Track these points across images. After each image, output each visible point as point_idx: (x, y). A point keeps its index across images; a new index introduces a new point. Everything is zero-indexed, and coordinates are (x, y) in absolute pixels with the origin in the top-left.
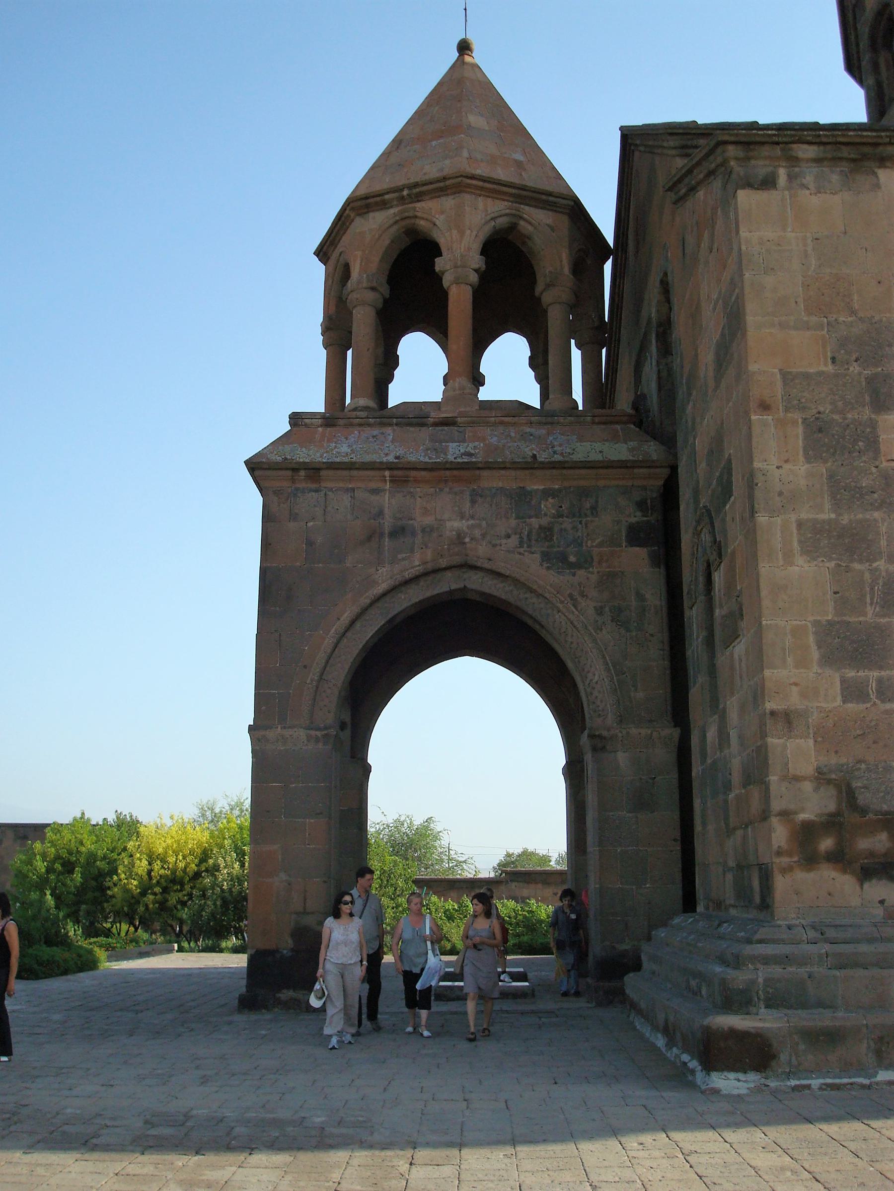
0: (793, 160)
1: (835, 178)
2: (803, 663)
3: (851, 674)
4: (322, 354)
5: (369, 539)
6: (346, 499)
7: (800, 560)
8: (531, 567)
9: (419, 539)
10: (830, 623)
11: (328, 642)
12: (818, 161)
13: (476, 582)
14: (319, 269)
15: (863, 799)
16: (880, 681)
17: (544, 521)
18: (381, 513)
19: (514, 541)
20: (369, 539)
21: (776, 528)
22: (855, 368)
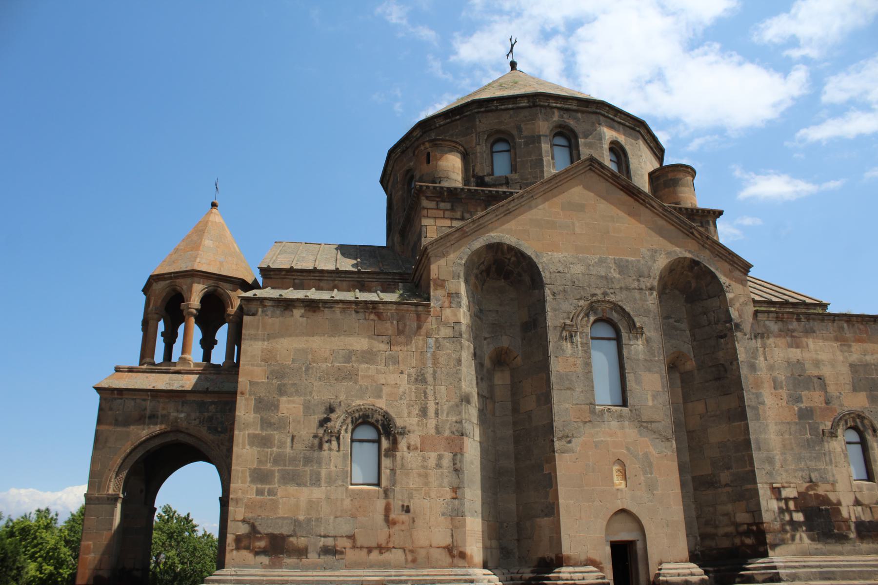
0: (265, 306)
1: (278, 312)
2: (243, 482)
3: (259, 486)
4: (140, 334)
5: (140, 419)
6: (132, 403)
7: (248, 447)
8: (204, 432)
9: (159, 420)
10: (255, 469)
11: (119, 461)
12: (273, 306)
13: (182, 438)
14: (143, 298)
15: (259, 528)
16: (269, 489)
17: (210, 414)
18: (146, 409)
19: (197, 422)
20: (140, 419)
21: (240, 436)
22: (274, 381)
